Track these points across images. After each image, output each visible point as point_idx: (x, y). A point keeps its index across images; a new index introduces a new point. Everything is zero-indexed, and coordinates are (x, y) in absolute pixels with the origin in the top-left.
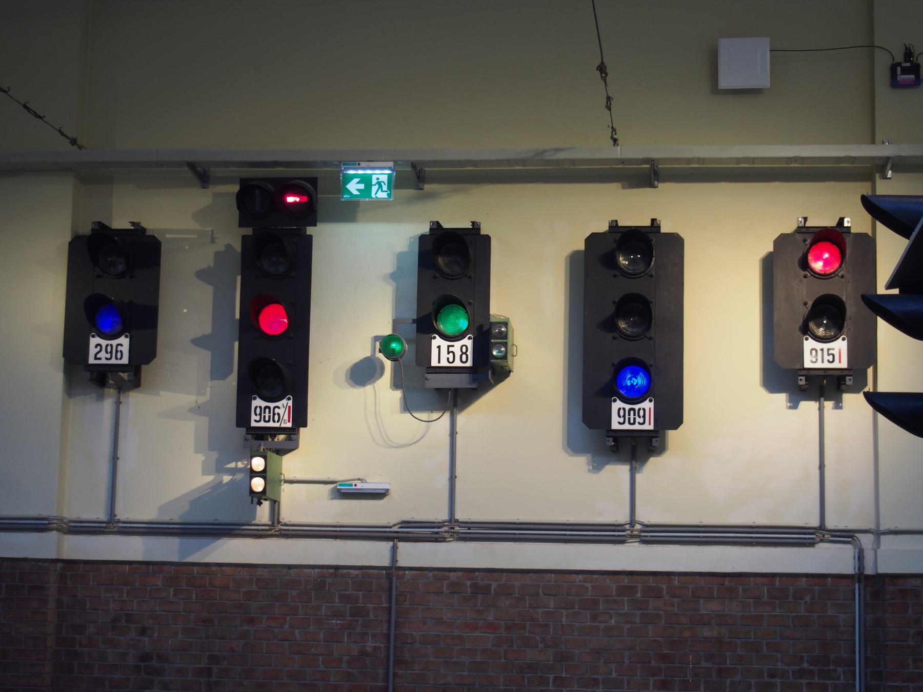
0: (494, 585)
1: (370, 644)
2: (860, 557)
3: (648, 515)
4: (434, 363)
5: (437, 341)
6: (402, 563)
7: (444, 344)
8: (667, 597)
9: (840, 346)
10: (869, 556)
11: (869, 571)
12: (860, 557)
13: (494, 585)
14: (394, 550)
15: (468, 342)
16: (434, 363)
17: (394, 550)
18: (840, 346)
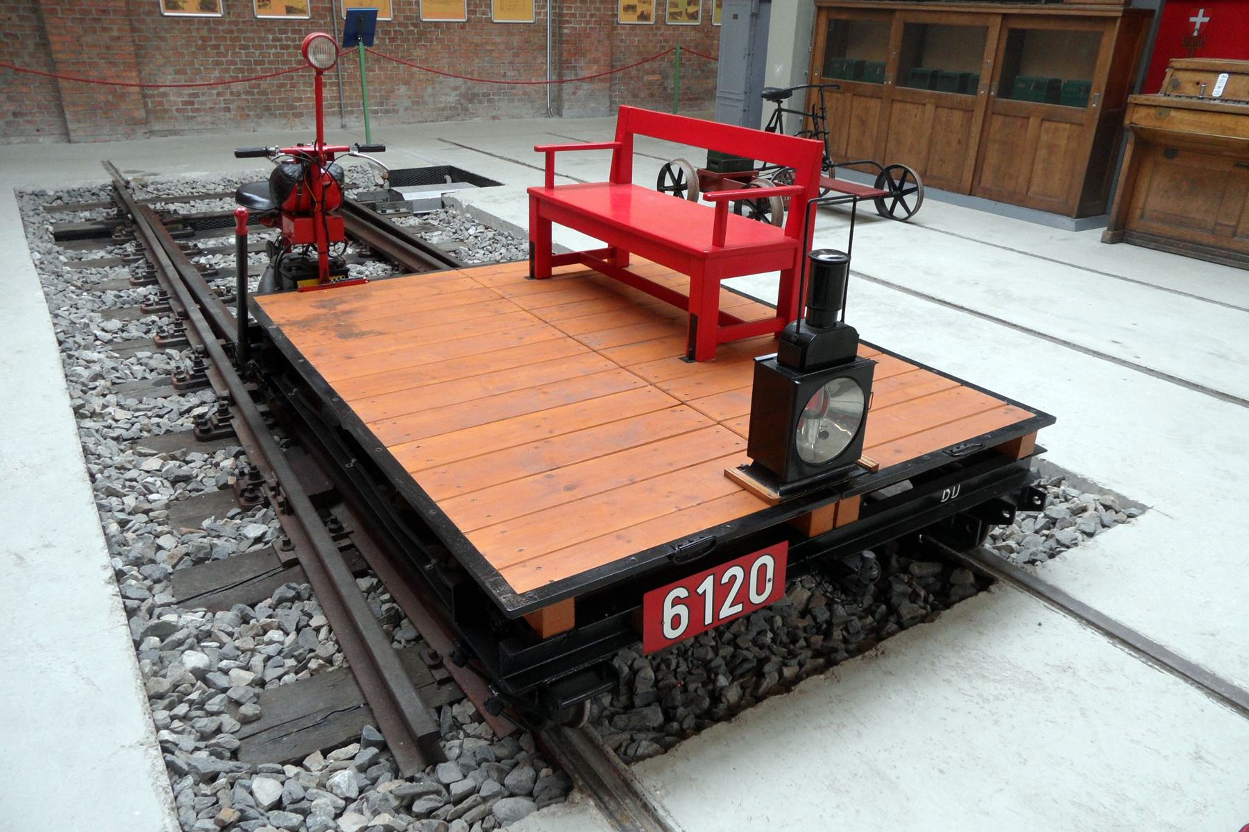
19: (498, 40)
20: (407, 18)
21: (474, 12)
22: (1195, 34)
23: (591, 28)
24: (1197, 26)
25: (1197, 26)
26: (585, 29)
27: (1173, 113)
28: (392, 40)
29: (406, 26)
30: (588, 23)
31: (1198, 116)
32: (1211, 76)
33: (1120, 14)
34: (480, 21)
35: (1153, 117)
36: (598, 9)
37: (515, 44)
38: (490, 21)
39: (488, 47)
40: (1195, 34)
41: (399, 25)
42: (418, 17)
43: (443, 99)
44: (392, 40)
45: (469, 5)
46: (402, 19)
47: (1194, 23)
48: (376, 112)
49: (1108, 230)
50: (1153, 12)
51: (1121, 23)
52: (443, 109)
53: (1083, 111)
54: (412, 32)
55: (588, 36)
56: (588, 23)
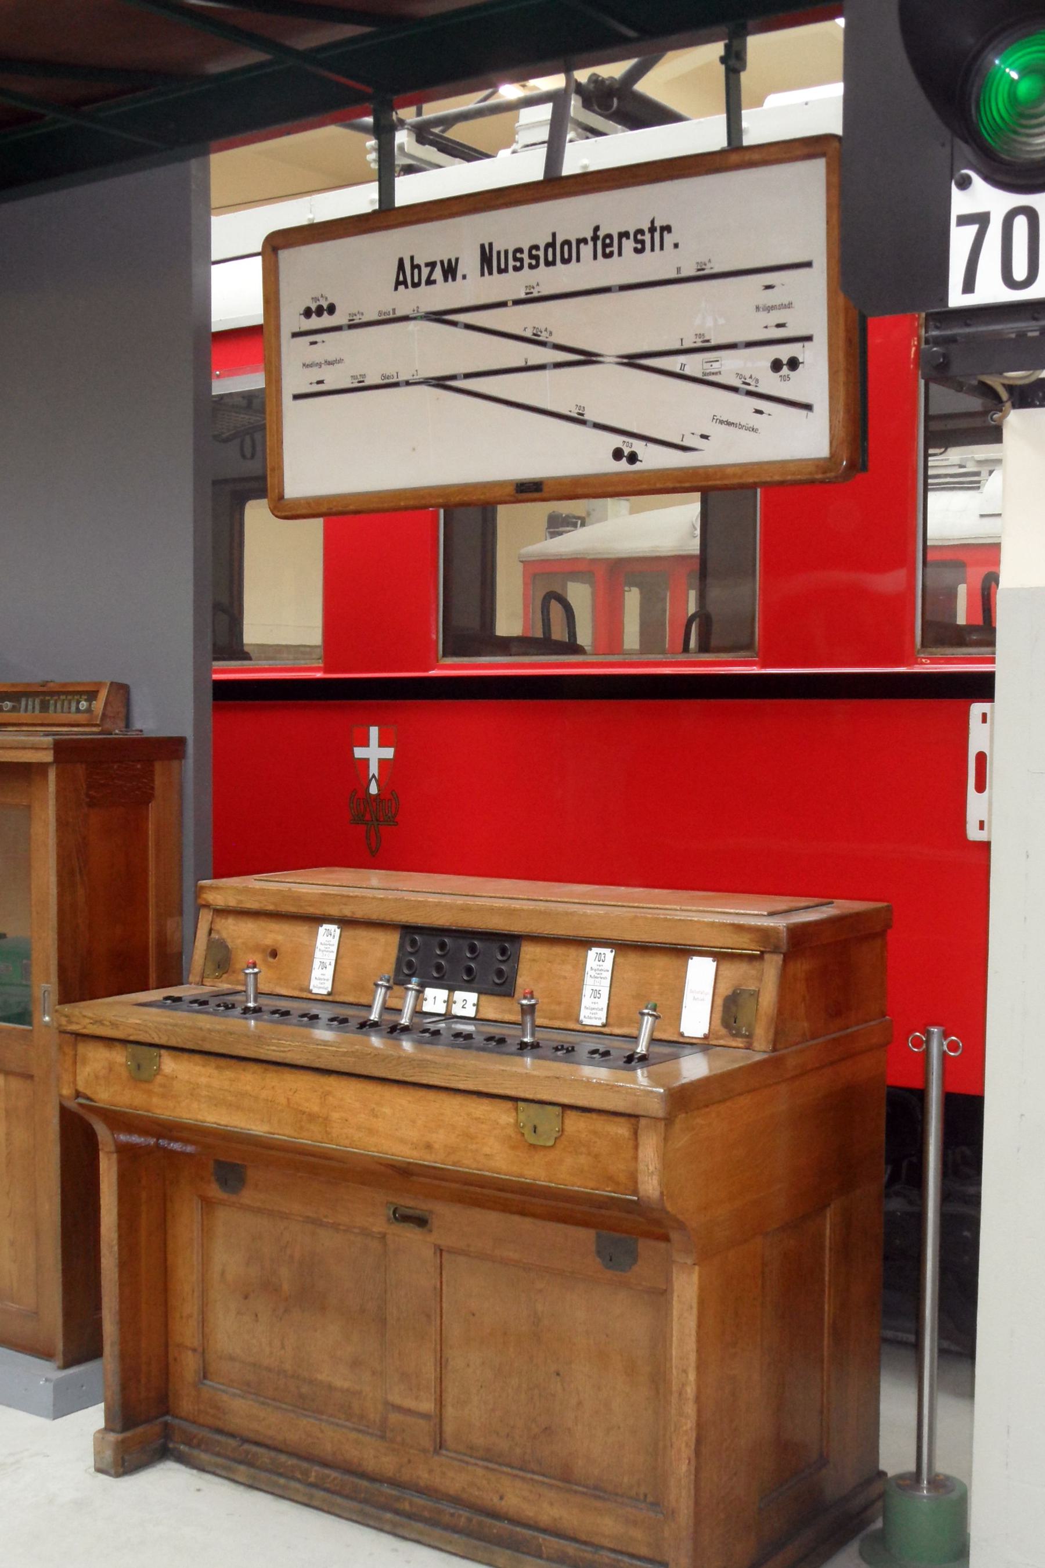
22: (373, 789)
24: (374, 769)
25: (374, 769)
27: (169, 1064)
31: (229, 1074)
32: (300, 930)
33: (48, 757)
35: (124, 1073)
40: (373, 789)
47: (365, 762)
49: (108, 1429)
50: (181, 741)
51: (58, 776)
53: (25, 1036)
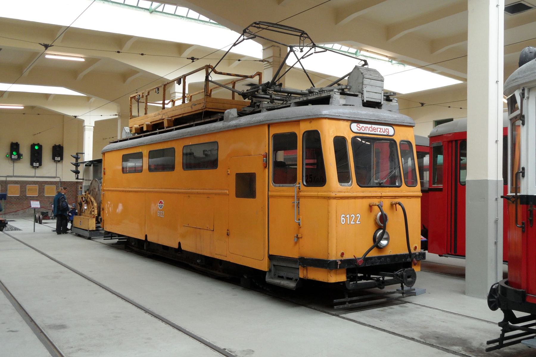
0: (18, 182)
1: (3, 189)
2: (60, 179)
3: (37, 175)
4: (12, 158)
5: (13, 156)
6: (7, 180)
7: (14, 156)
8: (39, 183)
9: (59, 158)
10: (61, 179)
11: (61, 181)
12: (60, 179)
13: (18, 182)
14: (6, 178)
15: (17, 156)
16: (12, 158)
17: (6, 178)
18: (59, 158)
19: (46, 200)
20: (23, 195)
21: (40, 194)
23: (70, 197)
26: (68, 197)
28: (19, 200)
29: (23, 197)
30: (69, 196)
34: (42, 196)
36: (72, 193)
37: (51, 201)
38: (44, 196)
39: (43, 201)
41: (21, 197)
42: (26, 195)
43: (31, 212)
44: (19, 200)
45: (39, 192)
46: (22, 196)
48: (13, 214)
52: (31, 214)
54: (24, 198)
55: (69, 199)
56: (69, 196)
